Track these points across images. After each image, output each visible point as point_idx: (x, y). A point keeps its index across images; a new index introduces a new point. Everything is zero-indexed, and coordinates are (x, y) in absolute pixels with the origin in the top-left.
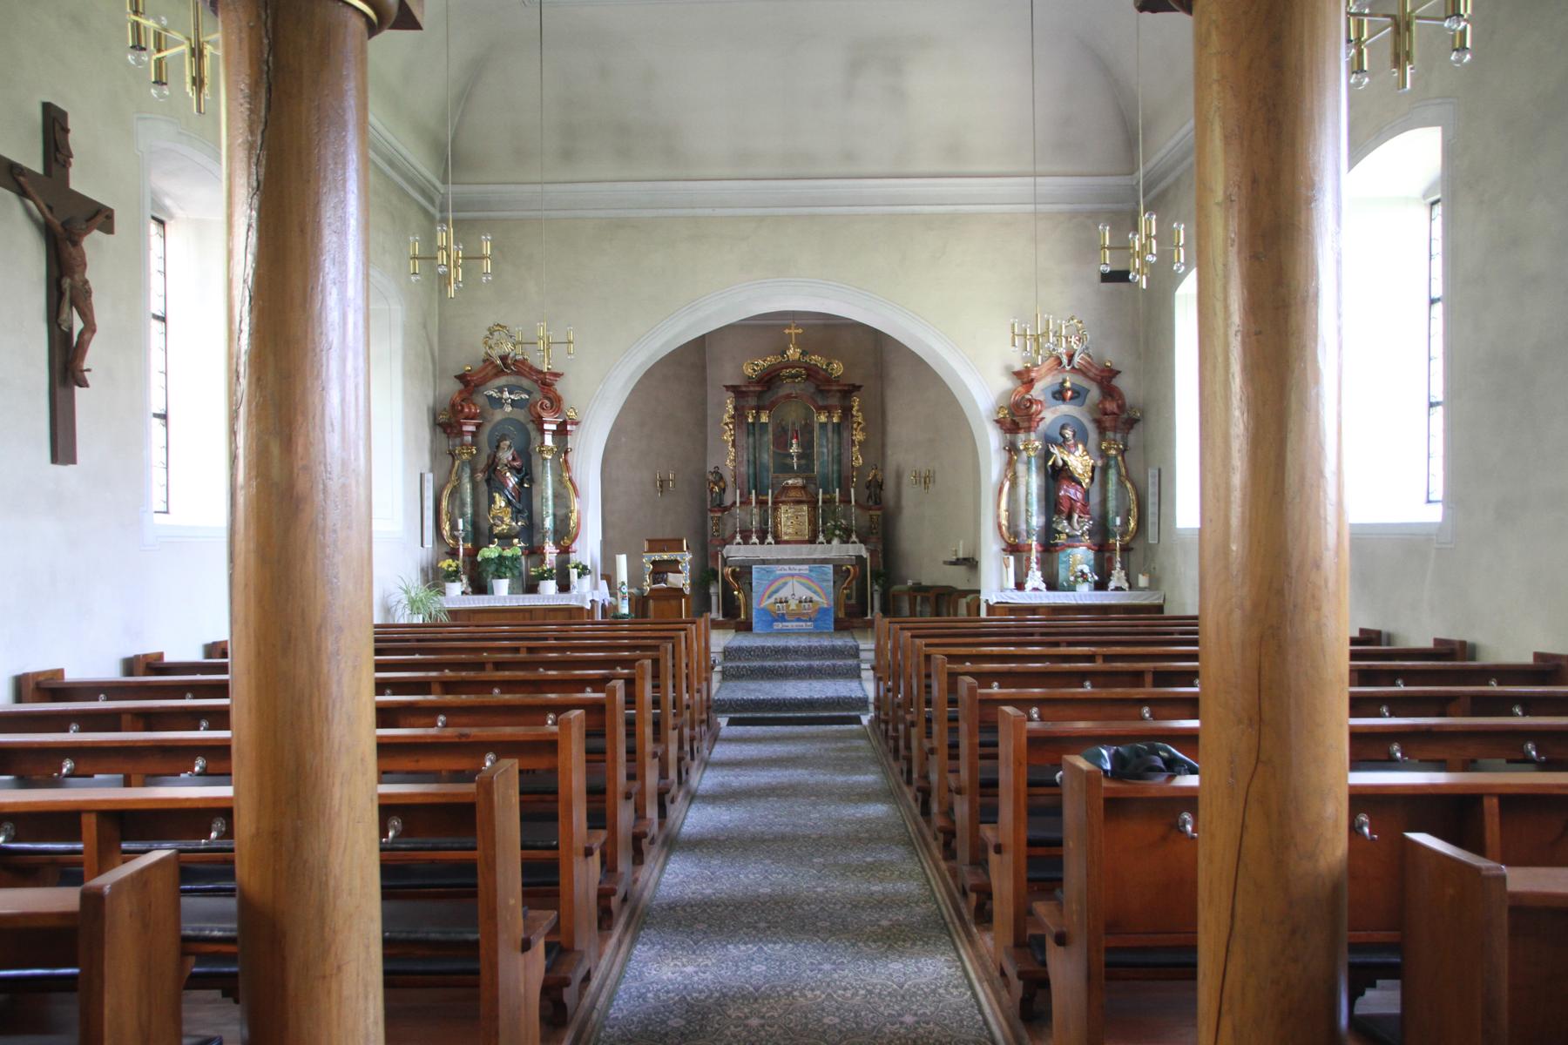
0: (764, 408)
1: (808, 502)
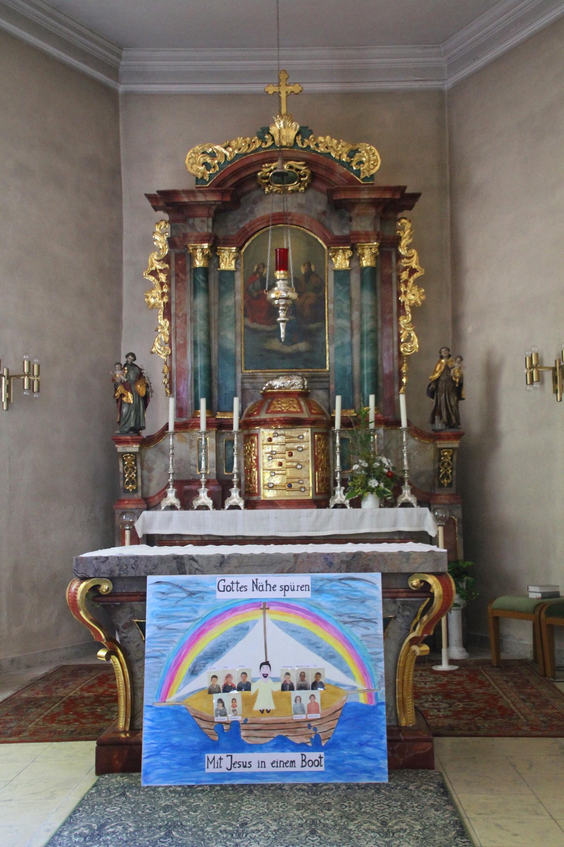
0: (227, 242)
1: (311, 423)
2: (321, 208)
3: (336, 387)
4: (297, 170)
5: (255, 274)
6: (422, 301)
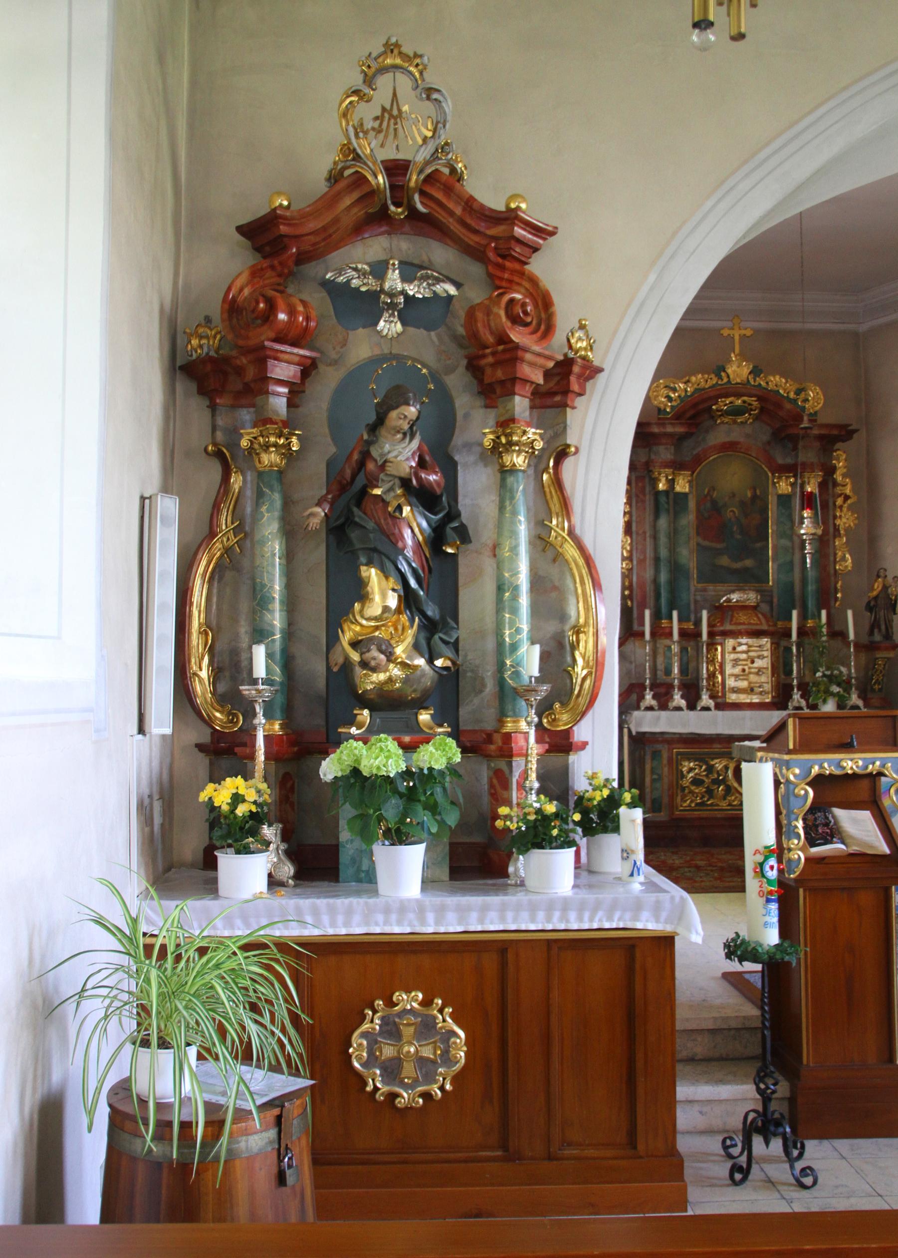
2: (765, 438)
3: (778, 601)
4: (750, 404)
5: (706, 496)
6: (855, 524)
